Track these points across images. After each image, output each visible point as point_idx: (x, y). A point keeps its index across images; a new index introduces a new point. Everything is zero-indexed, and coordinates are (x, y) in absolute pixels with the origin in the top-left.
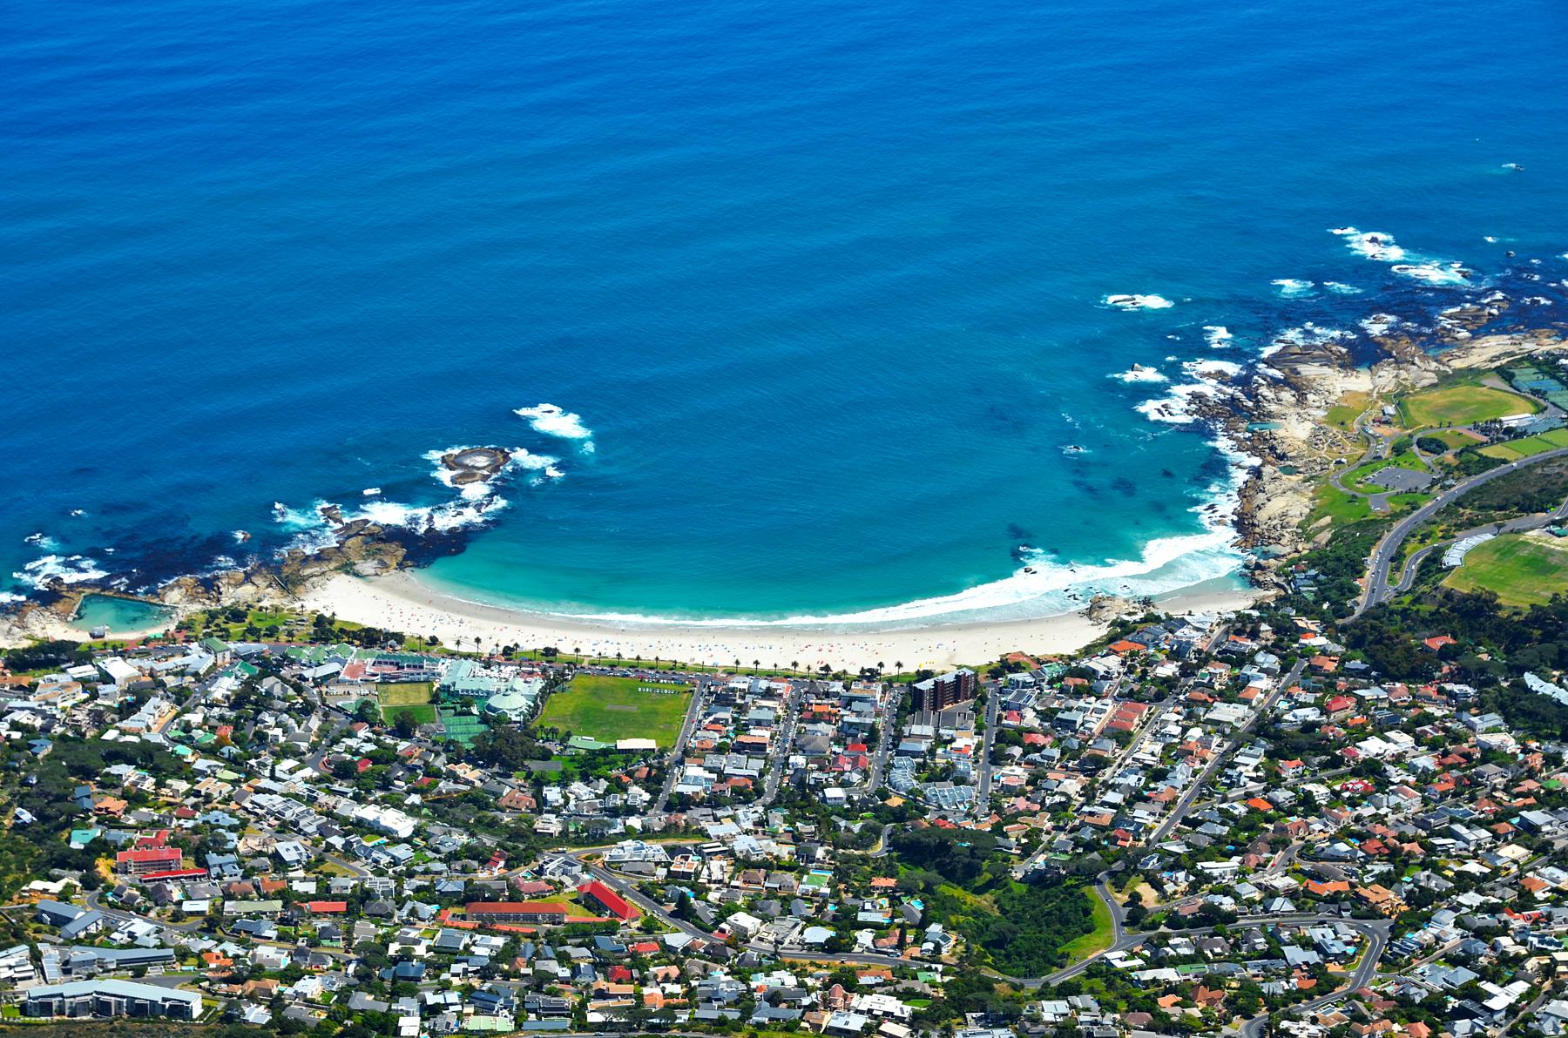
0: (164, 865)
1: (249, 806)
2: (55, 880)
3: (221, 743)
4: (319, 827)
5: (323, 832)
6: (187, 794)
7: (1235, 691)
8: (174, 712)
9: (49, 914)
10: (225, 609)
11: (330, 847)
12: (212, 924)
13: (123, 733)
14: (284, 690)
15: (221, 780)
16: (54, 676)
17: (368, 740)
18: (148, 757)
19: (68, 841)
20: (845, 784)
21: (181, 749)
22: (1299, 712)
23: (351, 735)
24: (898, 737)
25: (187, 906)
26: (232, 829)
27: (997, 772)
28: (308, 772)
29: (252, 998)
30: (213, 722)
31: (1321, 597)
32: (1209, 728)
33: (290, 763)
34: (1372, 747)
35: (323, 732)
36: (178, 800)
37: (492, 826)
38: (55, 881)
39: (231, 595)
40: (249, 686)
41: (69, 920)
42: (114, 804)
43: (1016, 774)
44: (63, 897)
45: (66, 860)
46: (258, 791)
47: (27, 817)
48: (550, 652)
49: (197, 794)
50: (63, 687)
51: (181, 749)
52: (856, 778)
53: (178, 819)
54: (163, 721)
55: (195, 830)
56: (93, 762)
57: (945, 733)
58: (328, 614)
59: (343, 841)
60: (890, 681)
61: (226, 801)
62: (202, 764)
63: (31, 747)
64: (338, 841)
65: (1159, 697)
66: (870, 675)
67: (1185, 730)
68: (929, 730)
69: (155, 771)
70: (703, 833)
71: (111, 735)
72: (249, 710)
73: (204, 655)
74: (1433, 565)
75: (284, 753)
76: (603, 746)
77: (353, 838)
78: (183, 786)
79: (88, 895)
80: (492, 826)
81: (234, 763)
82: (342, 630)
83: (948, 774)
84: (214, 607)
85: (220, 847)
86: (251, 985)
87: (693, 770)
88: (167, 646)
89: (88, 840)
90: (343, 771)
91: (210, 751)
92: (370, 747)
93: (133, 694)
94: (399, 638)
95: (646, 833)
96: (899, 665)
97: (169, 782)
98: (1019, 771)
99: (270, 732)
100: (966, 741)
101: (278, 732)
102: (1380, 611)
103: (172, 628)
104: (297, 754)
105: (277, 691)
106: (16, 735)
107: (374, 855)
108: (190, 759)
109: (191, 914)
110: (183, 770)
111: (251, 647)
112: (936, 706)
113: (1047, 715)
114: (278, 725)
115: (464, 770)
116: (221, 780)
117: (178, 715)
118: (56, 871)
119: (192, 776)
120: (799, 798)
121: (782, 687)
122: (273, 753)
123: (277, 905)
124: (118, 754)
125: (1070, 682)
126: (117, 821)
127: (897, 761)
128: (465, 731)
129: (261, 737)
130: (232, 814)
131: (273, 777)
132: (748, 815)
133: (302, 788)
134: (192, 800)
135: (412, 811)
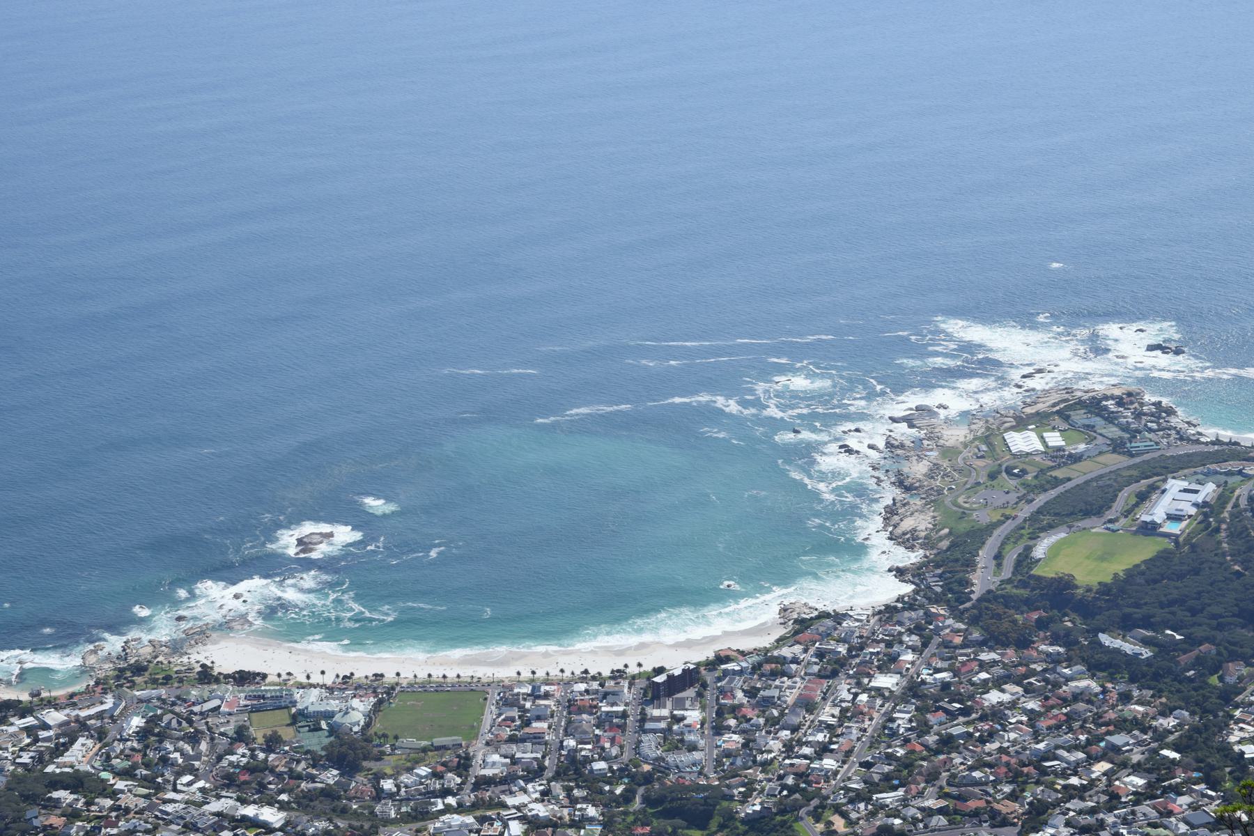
3: (134, 767)
6: (112, 809)
7: (889, 663)
14: (179, 723)
18: (76, 782)
21: (104, 775)
22: (938, 676)
30: (127, 752)
31: (947, 588)
34: (994, 697)
40: (152, 721)
46: (166, 802)
48: (378, 676)
50: (11, 735)
51: (104, 775)
58: (209, 664)
62: (121, 785)
66: (618, 675)
67: (856, 695)
68: (665, 712)
70: (504, 806)
74: (1025, 560)
78: (108, 803)
80: (344, 812)
81: (148, 781)
95: (460, 809)
96: (640, 665)
98: (735, 737)
101: (177, 755)
102: (989, 596)
103: (92, 683)
113: (751, 693)
114: (176, 750)
119: (114, 794)
120: (573, 769)
124: (57, 782)
125: (767, 668)
127: (644, 738)
128: (317, 742)
129: (165, 760)
131: (175, 790)
132: (535, 788)
135: (283, 806)
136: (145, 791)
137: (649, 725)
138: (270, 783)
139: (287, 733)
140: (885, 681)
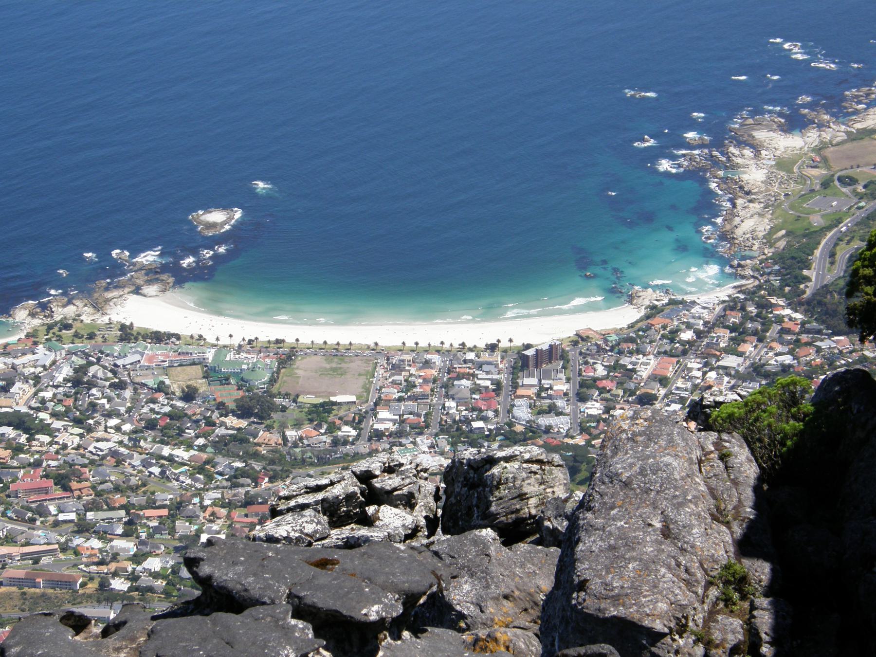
1: (94, 451)
6: (51, 444)
10: (56, 323)
12: (83, 528)
14: (104, 373)
15: (72, 434)
20: (485, 419)
21: (42, 415)
22: (779, 358)
24: (515, 386)
25: (62, 517)
27: (582, 407)
29: (115, 574)
30: (59, 397)
32: (721, 371)
36: (44, 449)
37: (256, 456)
39: (60, 313)
40: (81, 370)
43: (594, 408)
46: (98, 440)
48: (278, 341)
51: (42, 415)
52: (490, 414)
53: (47, 460)
54: (25, 398)
57: (546, 383)
58: (128, 323)
60: (505, 351)
62: (57, 424)
65: (684, 353)
66: (492, 348)
67: (705, 373)
68: (534, 381)
69: (26, 430)
73: (47, 352)
76: (321, 400)
80: (256, 456)
81: (78, 422)
82: (139, 334)
83: (553, 410)
84: (49, 321)
86: (113, 566)
87: (383, 414)
90: (151, 425)
92: (167, 409)
94: (178, 337)
96: (511, 340)
97: (37, 437)
98: (597, 405)
100: (561, 386)
101: (104, 401)
102: (825, 289)
103: (22, 336)
104: (118, 415)
105: (100, 374)
108: (49, 421)
109: (66, 522)
110: (45, 429)
111: (79, 345)
112: (537, 365)
115: (232, 421)
117: (36, 394)
121: (436, 358)
122: (103, 415)
123: (123, 513)
125: (624, 346)
127: (517, 402)
128: (230, 395)
129: (93, 406)
130: (83, 456)
132: (424, 442)
137: (520, 392)
138: (188, 428)
139: (202, 386)
140: (730, 361)
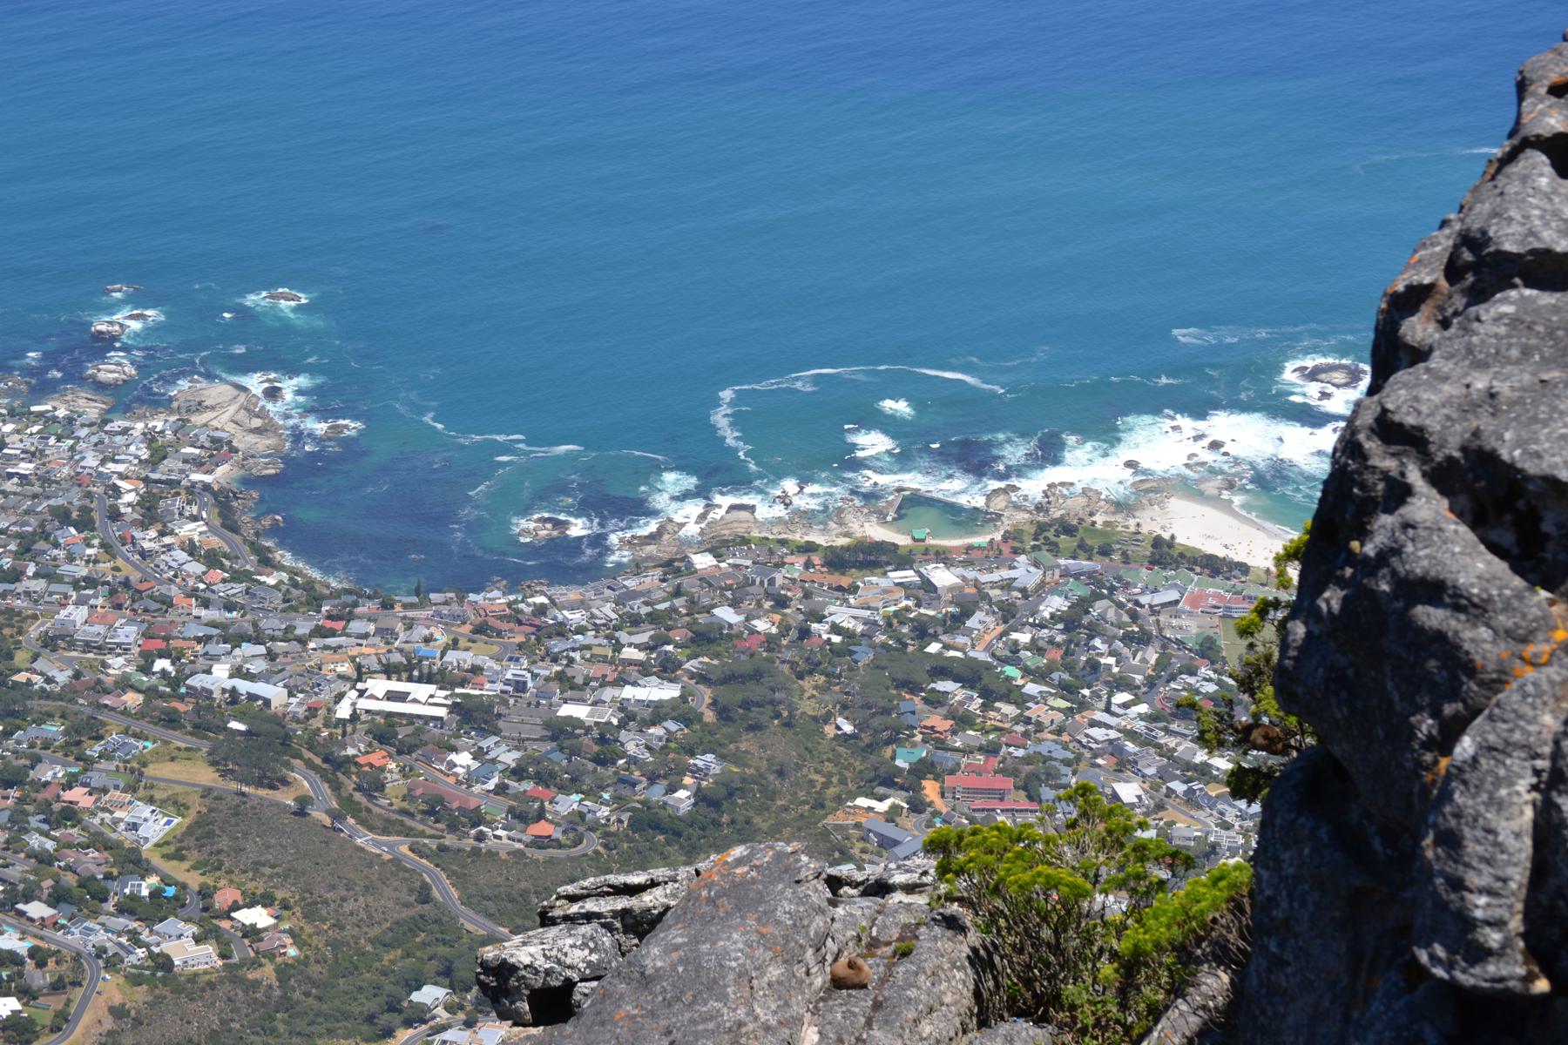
0: (988, 792)
1: (1084, 741)
2: (881, 799)
3: (1051, 668)
4: (1159, 769)
5: (1163, 775)
6: (1016, 720)
8: (1001, 628)
9: (876, 834)
11: (1170, 791)
13: (947, 647)
14: (1118, 616)
15: (1052, 708)
16: (874, 579)
17: (1210, 680)
18: (970, 675)
19: (893, 758)
21: (1011, 671)
23: (1193, 673)
26: (1067, 763)
28: (1143, 708)
33: (1121, 697)
35: (1162, 664)
36: (1007, 725)
38: (881, 800)
40: (1082, 605)
41: (896, 843)
42: (943, 725)
44: (892, 816)
45: (888, 780)
46: (1094, 724)
47: (848, 728)
49: (1028, 721)
50: (886, 591)
51: (1011, 671)
53: (1008, 745)
55: (1027, 760)
56: (919, 676)
58: (1166, 536)
59: (1184, 787)
61: (1059, 732)
62: (1032, 688)
63: (851, 653)
64: (1179, 787)
71: (934, 648)
72: (1083, 634)
73: (1032, 569)
75: (1120, 684)
77: (1196, 786)
79: (914, 818)
81: (1067, 690)
82: (1182, 555)
85: (1051, 777)
88: (994, 556)
89: (914, 760)
90: (1186, 709)
91: (1038, 675)
93: (957, 605)
97: (997, 704)
99: (1103, 661)
103: (998, 537)
105: (1111, 614)
106: (836, 639)
107: (1220, 807)
110: (1013, 694)
111: (1085, 564)
114: (1111, 654)
116: (1052, 708)
117: (1005, 633)
118: (881, 790)
119: (1021, 700)
122: (1107, 683)
124: (942, 670)
126: (943, 742)
129: (1094, 666)
130: (1065, 747)
131: (1108, 710)
133: (1140, 726)
134: (1020, 728)
136: (1064, 704)
